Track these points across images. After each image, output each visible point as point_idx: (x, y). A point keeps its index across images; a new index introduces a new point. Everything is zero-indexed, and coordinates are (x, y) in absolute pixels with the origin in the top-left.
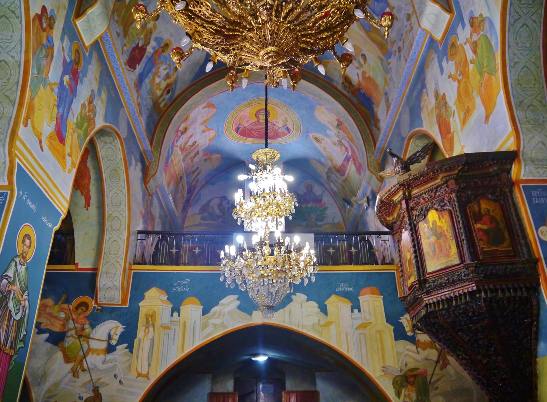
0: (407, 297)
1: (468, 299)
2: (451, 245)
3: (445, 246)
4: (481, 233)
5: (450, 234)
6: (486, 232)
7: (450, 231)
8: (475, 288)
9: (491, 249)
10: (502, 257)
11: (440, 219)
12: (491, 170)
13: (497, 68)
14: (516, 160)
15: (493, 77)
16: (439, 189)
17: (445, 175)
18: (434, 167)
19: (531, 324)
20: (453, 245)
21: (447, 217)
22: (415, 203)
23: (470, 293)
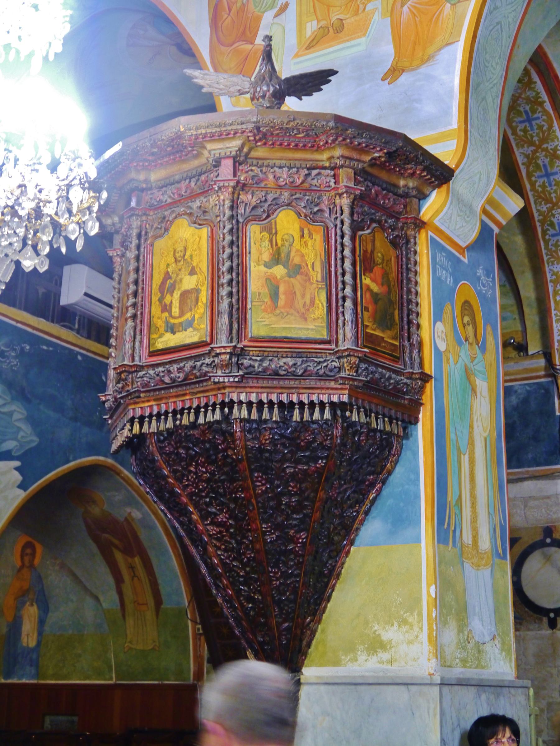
0: (141, 368)
1: (327, 415)
2: (317, 298)
3: (303, 296)
4: (368, 295)
5: (319, 276)
6: (375, 297)
7: (318, 268)
8: (345, 399)
9: (377, 333)
10: (384, 353)
11: (302, 236)
12: (402, 183)
14: (445, 186)
15: (448, 5)
16: (314, 172)
17: (347, 153)
18: (347, 130)
19: (372, 485)
20: (320, 301)
21: (319, 238)
22: (253, 177)
23: (333, 405)
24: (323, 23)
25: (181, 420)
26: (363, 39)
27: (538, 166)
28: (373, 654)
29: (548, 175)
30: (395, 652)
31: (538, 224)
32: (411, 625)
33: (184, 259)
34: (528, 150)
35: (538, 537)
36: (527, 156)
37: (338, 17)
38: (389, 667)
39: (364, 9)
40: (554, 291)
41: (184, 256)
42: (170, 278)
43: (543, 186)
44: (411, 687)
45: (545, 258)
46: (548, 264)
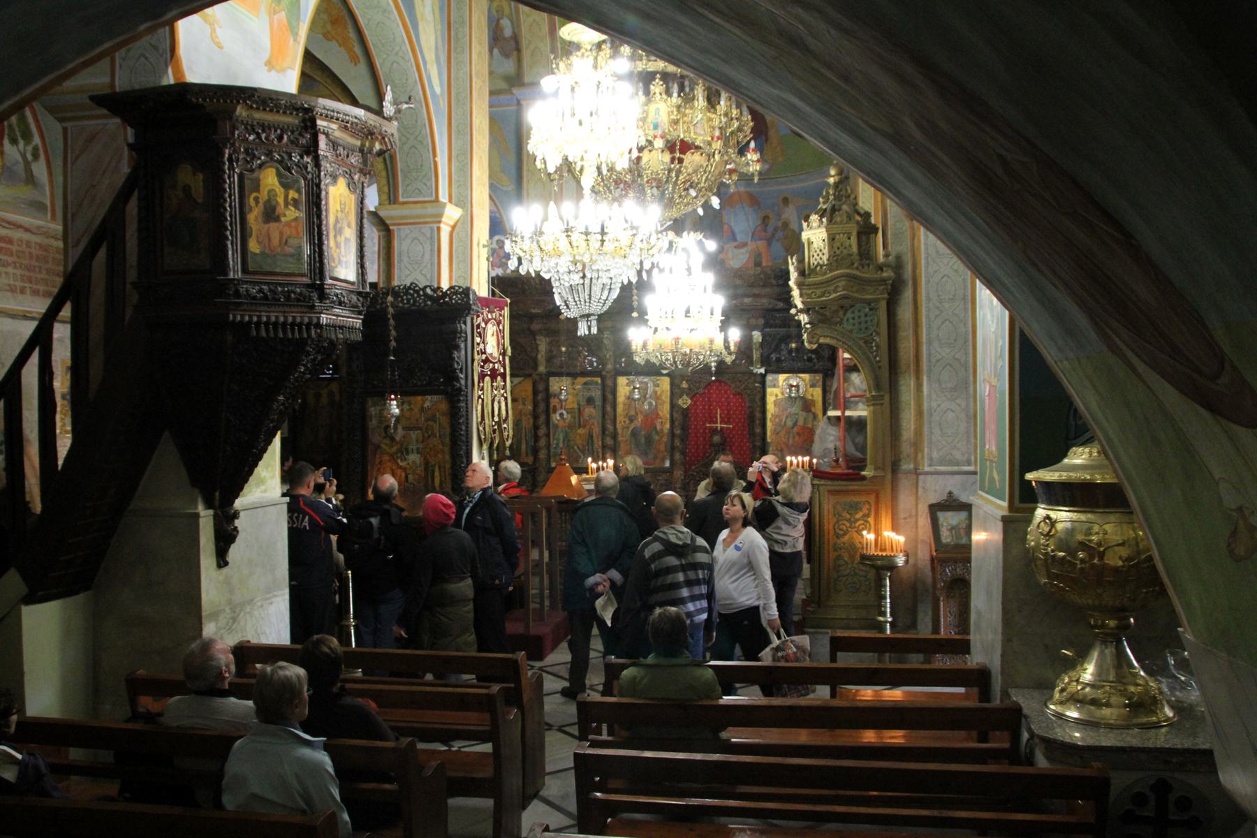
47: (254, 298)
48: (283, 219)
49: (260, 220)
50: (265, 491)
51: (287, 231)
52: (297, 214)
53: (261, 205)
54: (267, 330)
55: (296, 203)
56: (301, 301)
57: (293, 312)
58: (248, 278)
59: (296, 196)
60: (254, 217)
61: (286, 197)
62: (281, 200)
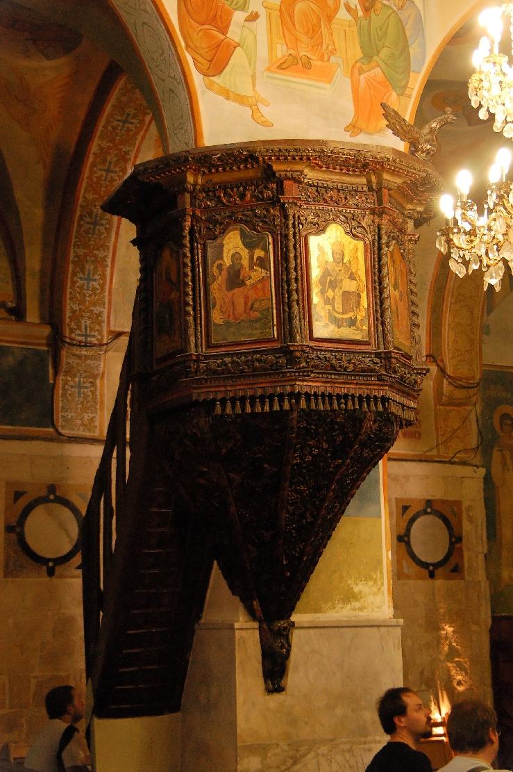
13: (407, 92)
15: (394, 94)
24: (291, 52)
25: (346, 404)
26: (329, 86)
27: (104, 161)
28: (348, 604)
29: (108, 171)
30: (364, 601)
31: (79, 208)
32: (375, 582)
33: (343, 263)
34: (105, 144)
35: (43, 493)
36: (101, 149)
37: (306, 53)
38: (360, 613)
39: (329, 60)
40: (73, 270)
41: (343, 259)
42: (330, 275)
43: (99, 178)
44: (380, 628)
45: (73, 240)
46: (74, 246)
47: (215, 372)
48: (248, 282)
49: (224, 288)
50: (361, 609)
51: (252, 294)
52: (263, 273)
53: (224, 273)
54: (233, 407)
55: (263, 263)
56: (268, 370)
57: (262, 383)
58: (213, 352)
59: (262, 254)
60: (217, 289)
61: (251, 258)
62: (245, 262)
